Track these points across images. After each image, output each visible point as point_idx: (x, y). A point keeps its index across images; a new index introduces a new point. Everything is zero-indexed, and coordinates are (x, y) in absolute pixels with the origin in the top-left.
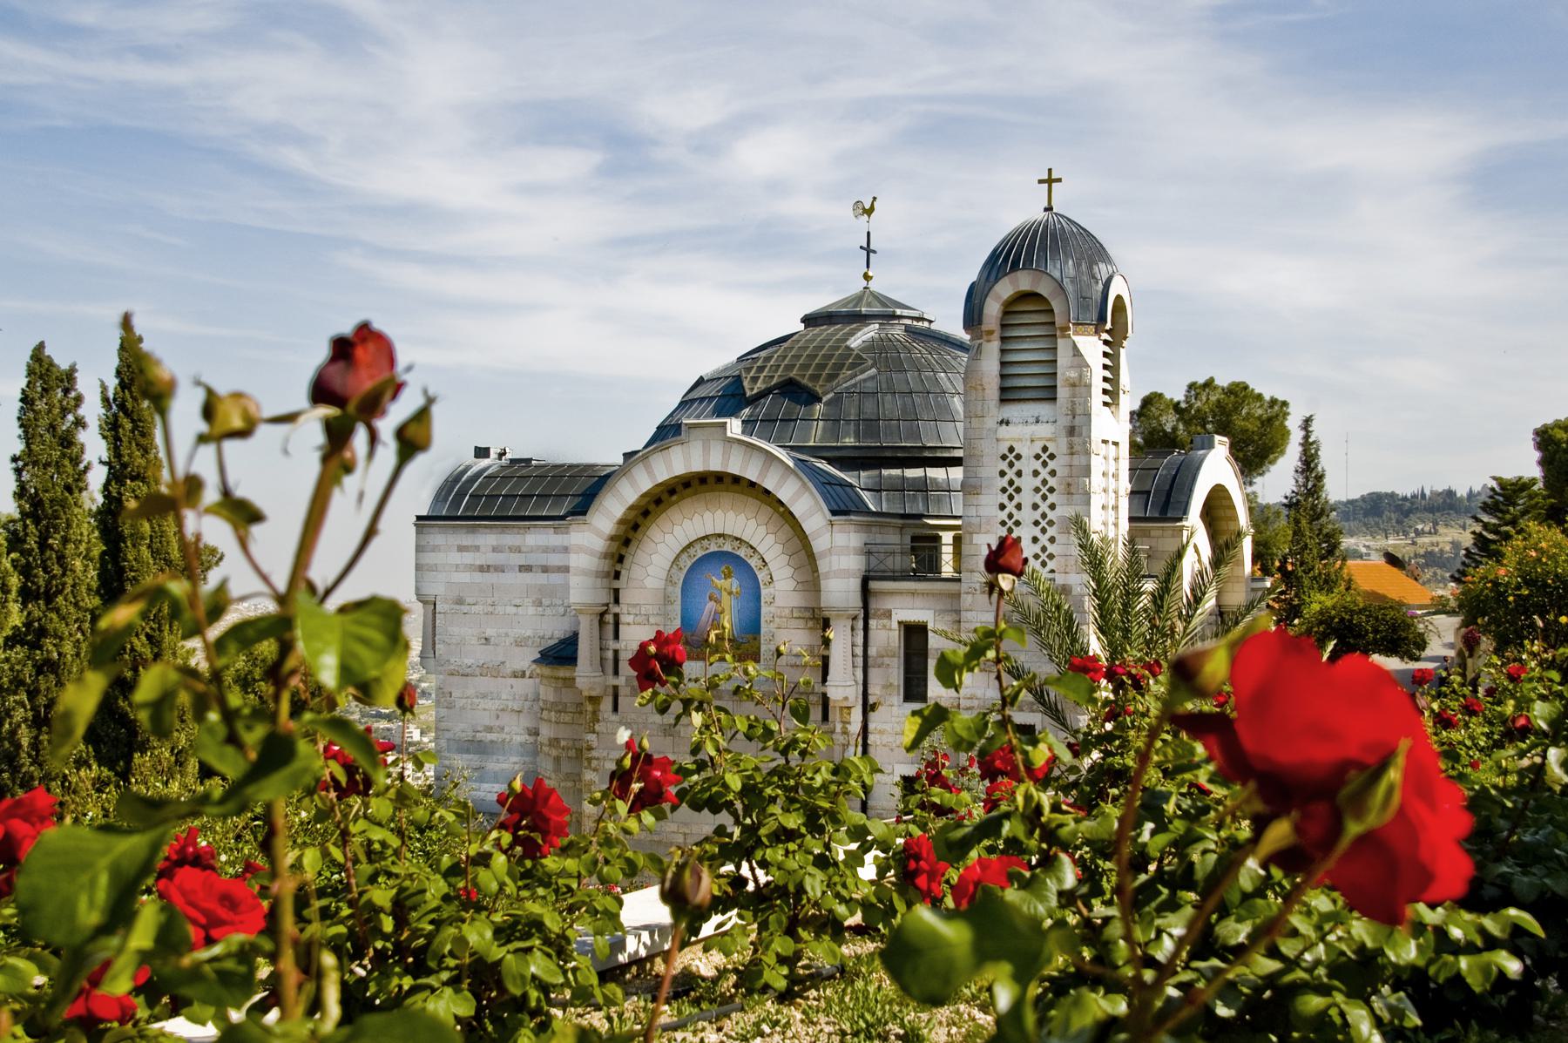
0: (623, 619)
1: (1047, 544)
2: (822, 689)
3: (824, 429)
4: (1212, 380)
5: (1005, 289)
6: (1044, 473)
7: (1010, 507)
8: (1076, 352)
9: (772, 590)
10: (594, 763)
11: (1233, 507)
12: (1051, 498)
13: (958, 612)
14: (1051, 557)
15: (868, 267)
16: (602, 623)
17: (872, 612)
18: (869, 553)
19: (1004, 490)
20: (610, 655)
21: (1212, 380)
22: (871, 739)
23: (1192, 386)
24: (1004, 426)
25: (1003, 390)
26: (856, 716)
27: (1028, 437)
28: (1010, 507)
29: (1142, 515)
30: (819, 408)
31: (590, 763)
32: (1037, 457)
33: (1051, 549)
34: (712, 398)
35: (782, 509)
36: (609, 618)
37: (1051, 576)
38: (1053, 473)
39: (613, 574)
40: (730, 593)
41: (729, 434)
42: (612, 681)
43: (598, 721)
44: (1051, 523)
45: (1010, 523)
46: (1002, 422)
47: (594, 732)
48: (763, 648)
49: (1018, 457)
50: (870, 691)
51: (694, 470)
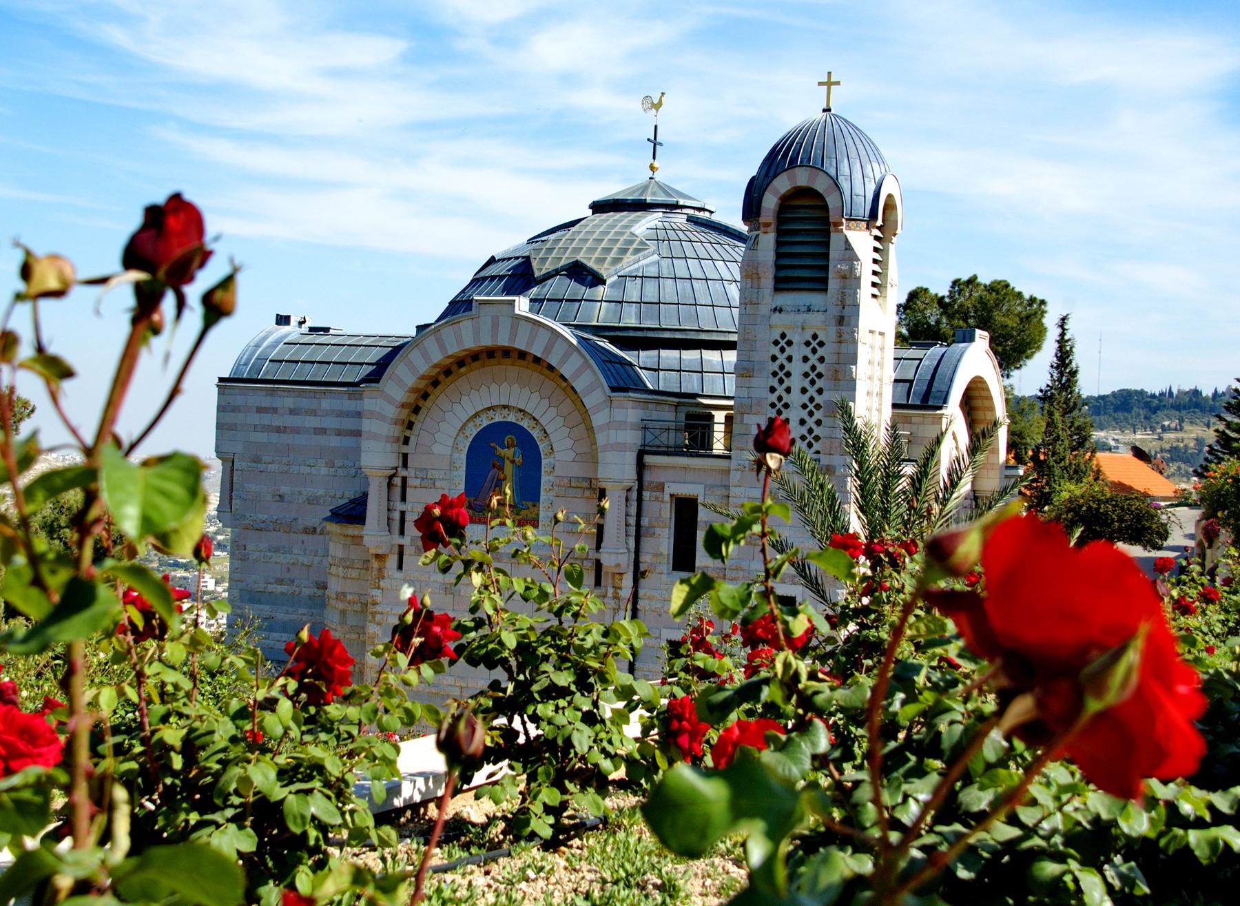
0: (410, 482)
1: (814, 427)
2: (596, 556)
3: (607, 310)
4: (975, 277)
5: (782, 184)
6: (813, 359)
7: (780, 390)
8: (848, 246)
9: (552, 460)
10: (378, 617)
11: (990, 398)
12: (819, 383)
13: (727, 487)
14: (817, 438)
15: (654, 158)
16: (390, 485)
17: (645, 484)
18: (645, 428)
19: (775, 374)
20: (397, 516)
21: (975, 277)
22: (641, 604)
23: (956, 283)
24: (777, 313)
25: (778, 280)
26: (628, 582)
27: (799, 324)
28: (780, 390)
29: (905, 402)
31: (374, 617)
32: (808, 344)
33: (817, 431)
34: (502, 277)
35: (564, 384)
36: (397, 481)
37: (816, 456)
38: (822, 360)
39: (402, 439)
40: (513, 462)
41: (517, 312)
42: (399, 540)
43: (383, 577)
44: (818, 407)
45: (779, 405)
46: (775, 310)
47: (379, 588)
48: (542, 514)
49: (790, 343)
50: (642, 559)
51: (483, 344)
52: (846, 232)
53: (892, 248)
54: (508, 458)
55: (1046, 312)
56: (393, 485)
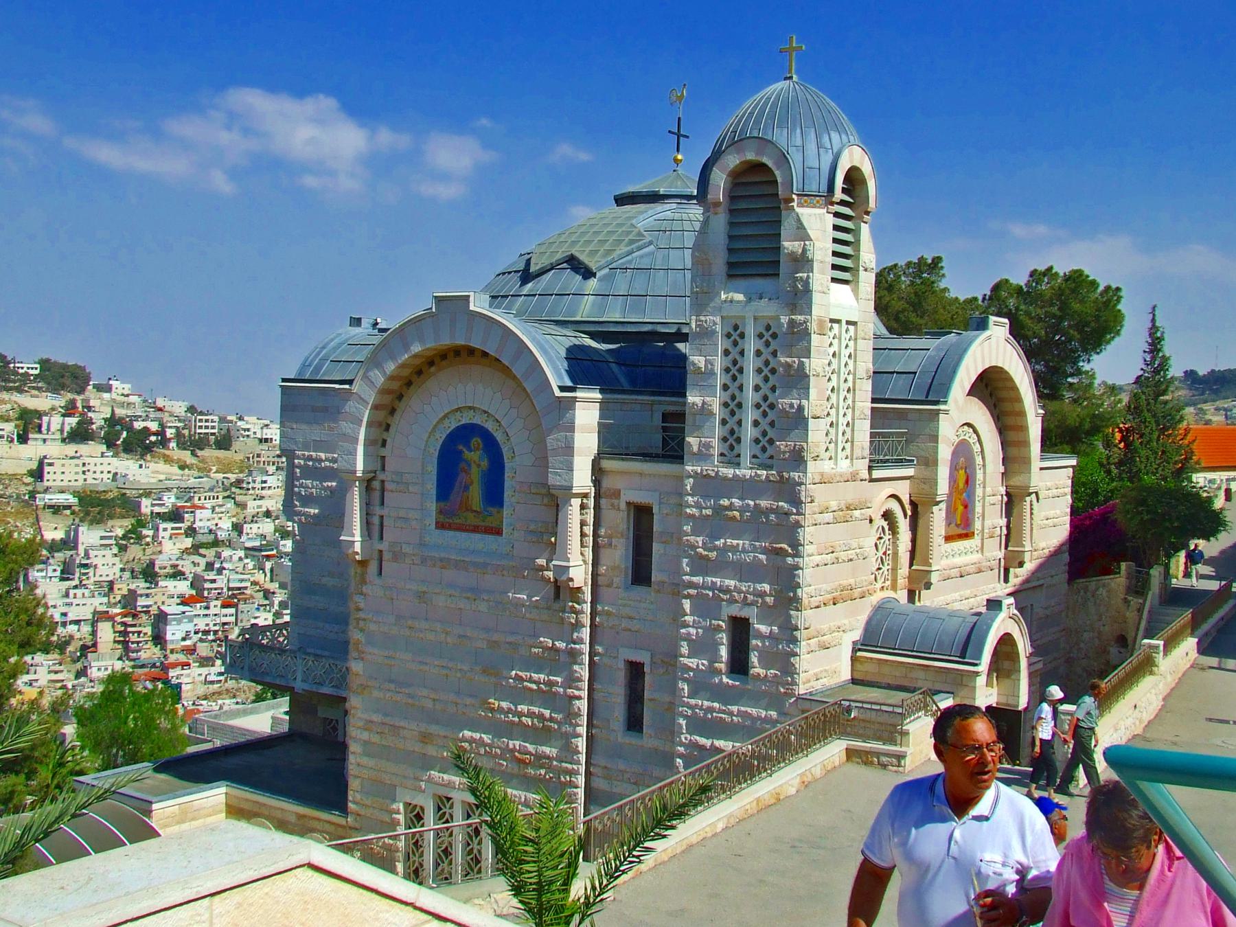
3: (594, 304)
4: (1051, 268)
5: (732, 161)
8: (800, 226)
10: (362, 624)
11: (1015, 389)
20: (376, 520)
21: (1051, 268)
23: (1033, 274)
25: (730, 265)
29: (924, 398)
30: (592, 284)
31: (358, 623)
34: (519, 271)
39: (380, 442)
40: (479, 466)
41: (472, 308)
47: (362, 594)
52: (798, 210)
53: (865, 230)
54: (475, 462)
55: (1121, 297)
56: (372, 489)
